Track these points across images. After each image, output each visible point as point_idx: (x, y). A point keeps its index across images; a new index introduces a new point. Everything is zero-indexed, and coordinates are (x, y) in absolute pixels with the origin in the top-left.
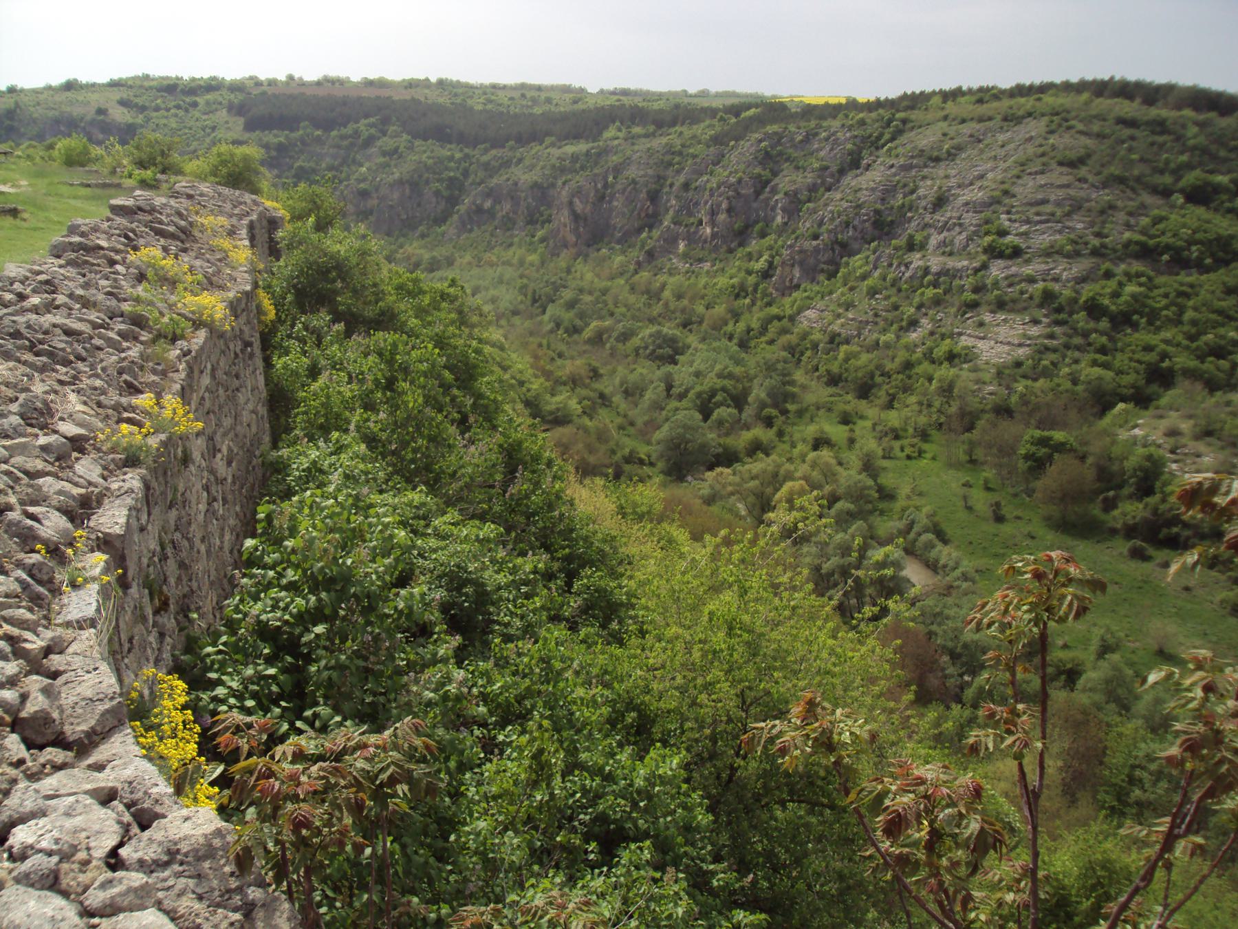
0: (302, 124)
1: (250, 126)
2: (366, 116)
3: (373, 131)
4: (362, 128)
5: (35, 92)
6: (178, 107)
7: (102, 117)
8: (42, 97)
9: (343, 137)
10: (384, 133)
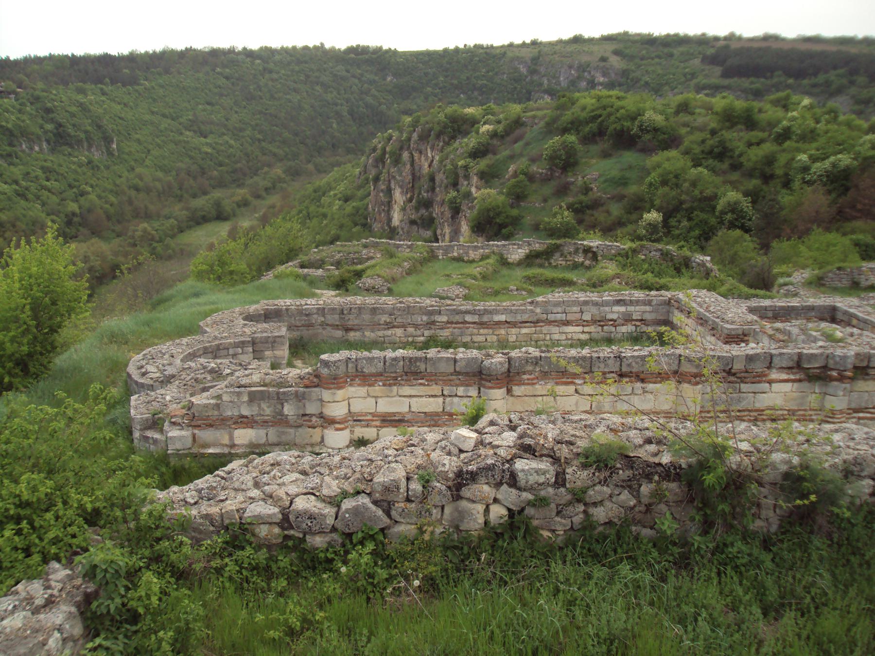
0: (777, 73)
1: (726, 74)
2: (835, 68)
3: (844, 81)
4: (833, 78)
5: (550, 44)
6: (659, 57)
7: (604, 64)
8: (557, 48)
9: (814, 86)
10: (852, 83)
